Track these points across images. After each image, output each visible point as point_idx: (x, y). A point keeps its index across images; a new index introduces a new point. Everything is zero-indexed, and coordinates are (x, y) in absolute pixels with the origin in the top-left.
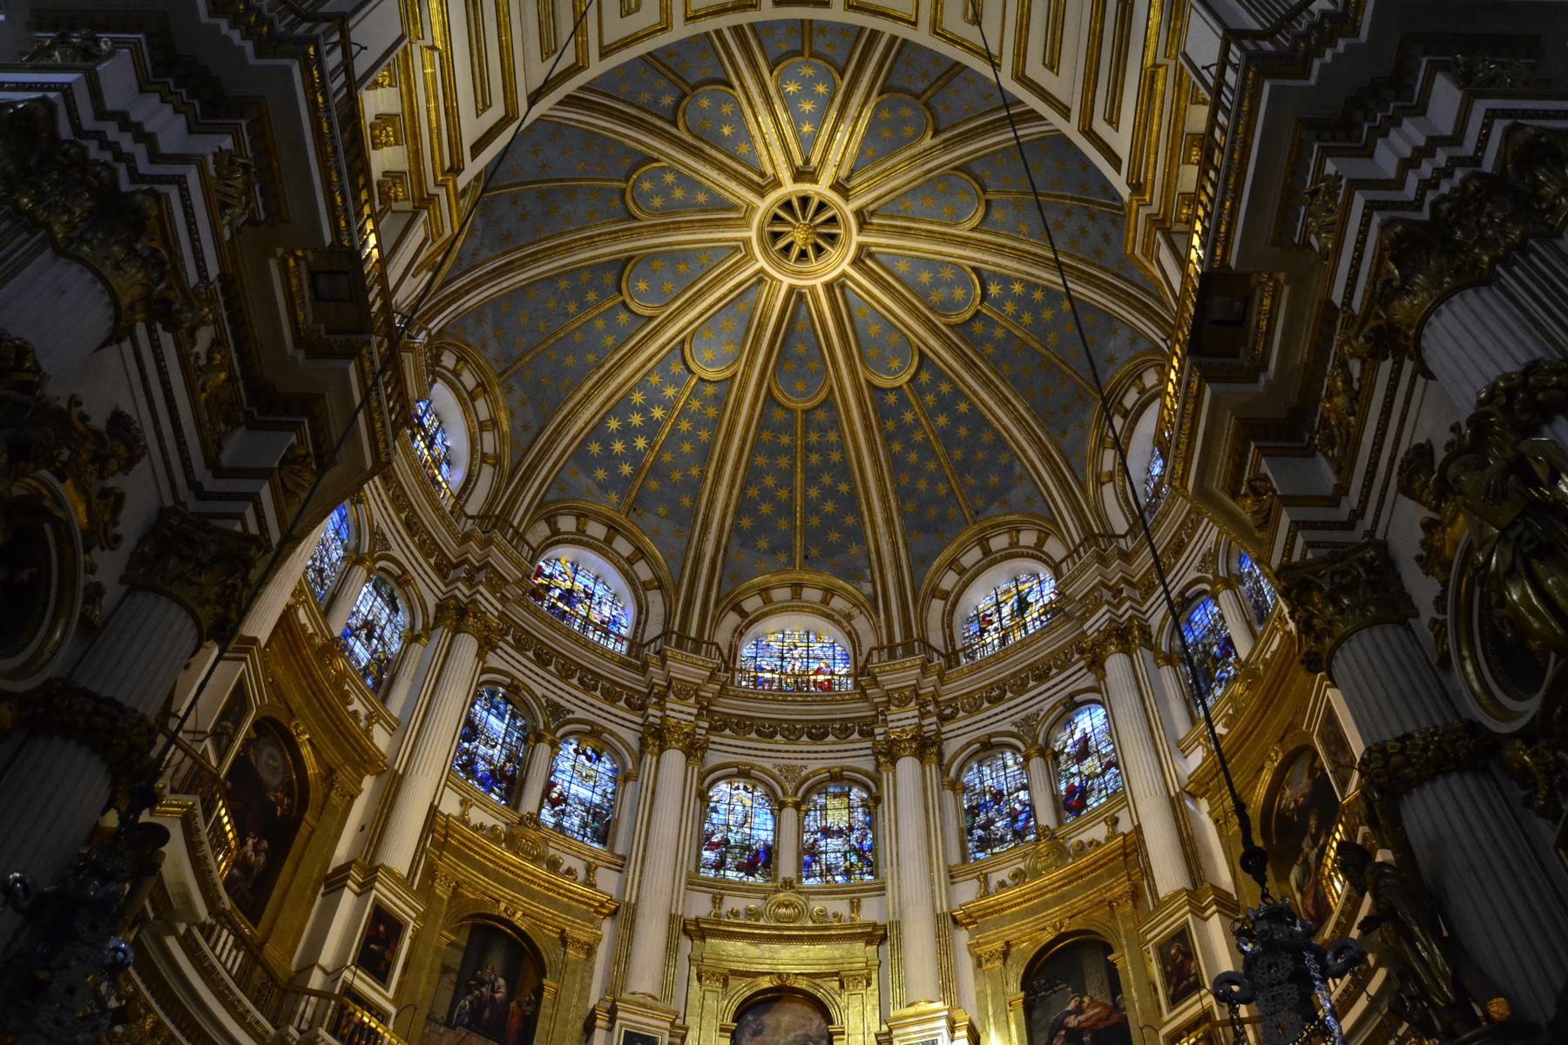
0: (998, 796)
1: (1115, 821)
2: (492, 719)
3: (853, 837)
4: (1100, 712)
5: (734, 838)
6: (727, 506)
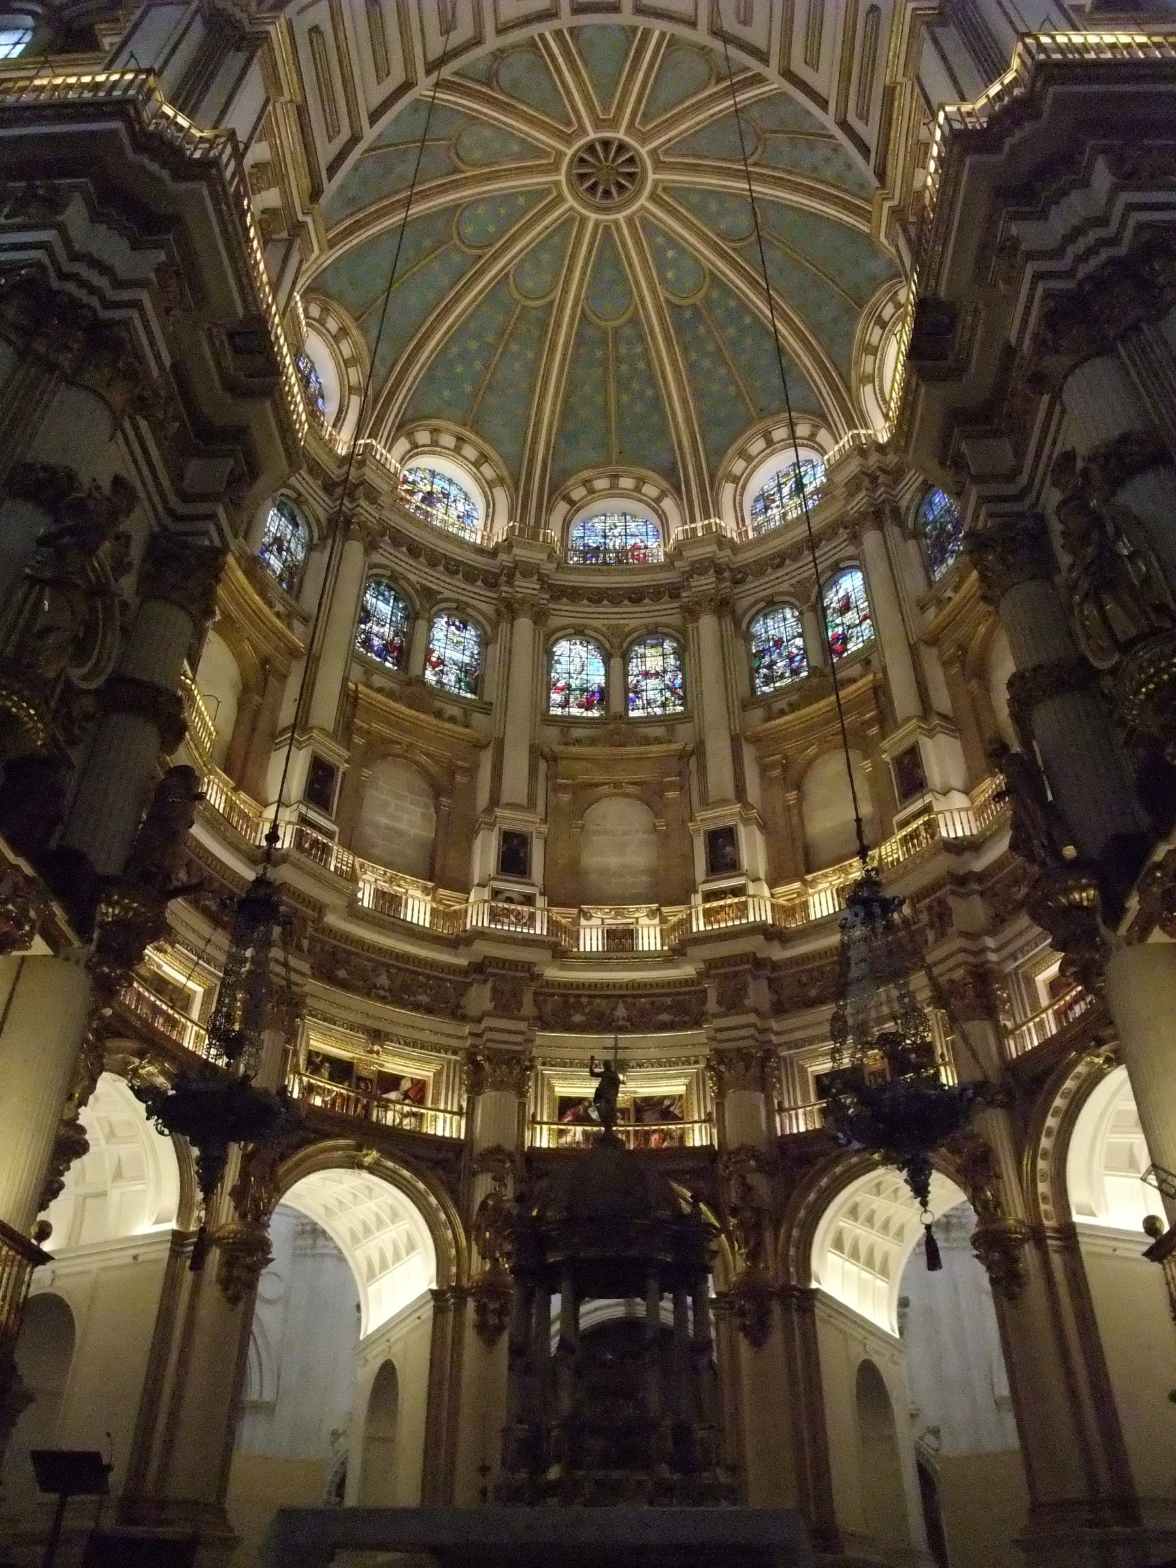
0: (779, 643)
1: (867, 663)
2: (381, 605)
3: (667, 678)
4: (858, 576)
5: (574, 683)
6: (553, 412)
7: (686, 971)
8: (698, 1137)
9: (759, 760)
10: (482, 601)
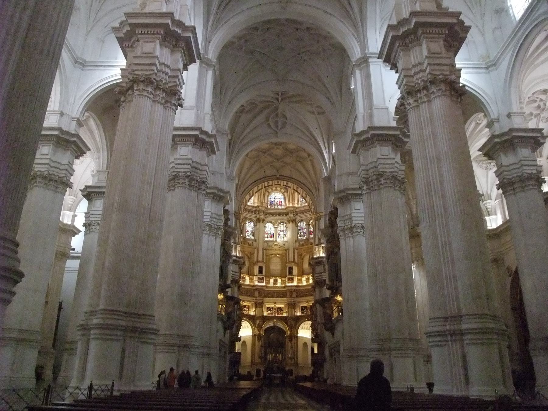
0: (302, 229)
7: (285, 289)
8: (285, 314)
9: (298, 253)
10: (253, 216)
